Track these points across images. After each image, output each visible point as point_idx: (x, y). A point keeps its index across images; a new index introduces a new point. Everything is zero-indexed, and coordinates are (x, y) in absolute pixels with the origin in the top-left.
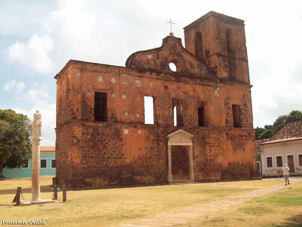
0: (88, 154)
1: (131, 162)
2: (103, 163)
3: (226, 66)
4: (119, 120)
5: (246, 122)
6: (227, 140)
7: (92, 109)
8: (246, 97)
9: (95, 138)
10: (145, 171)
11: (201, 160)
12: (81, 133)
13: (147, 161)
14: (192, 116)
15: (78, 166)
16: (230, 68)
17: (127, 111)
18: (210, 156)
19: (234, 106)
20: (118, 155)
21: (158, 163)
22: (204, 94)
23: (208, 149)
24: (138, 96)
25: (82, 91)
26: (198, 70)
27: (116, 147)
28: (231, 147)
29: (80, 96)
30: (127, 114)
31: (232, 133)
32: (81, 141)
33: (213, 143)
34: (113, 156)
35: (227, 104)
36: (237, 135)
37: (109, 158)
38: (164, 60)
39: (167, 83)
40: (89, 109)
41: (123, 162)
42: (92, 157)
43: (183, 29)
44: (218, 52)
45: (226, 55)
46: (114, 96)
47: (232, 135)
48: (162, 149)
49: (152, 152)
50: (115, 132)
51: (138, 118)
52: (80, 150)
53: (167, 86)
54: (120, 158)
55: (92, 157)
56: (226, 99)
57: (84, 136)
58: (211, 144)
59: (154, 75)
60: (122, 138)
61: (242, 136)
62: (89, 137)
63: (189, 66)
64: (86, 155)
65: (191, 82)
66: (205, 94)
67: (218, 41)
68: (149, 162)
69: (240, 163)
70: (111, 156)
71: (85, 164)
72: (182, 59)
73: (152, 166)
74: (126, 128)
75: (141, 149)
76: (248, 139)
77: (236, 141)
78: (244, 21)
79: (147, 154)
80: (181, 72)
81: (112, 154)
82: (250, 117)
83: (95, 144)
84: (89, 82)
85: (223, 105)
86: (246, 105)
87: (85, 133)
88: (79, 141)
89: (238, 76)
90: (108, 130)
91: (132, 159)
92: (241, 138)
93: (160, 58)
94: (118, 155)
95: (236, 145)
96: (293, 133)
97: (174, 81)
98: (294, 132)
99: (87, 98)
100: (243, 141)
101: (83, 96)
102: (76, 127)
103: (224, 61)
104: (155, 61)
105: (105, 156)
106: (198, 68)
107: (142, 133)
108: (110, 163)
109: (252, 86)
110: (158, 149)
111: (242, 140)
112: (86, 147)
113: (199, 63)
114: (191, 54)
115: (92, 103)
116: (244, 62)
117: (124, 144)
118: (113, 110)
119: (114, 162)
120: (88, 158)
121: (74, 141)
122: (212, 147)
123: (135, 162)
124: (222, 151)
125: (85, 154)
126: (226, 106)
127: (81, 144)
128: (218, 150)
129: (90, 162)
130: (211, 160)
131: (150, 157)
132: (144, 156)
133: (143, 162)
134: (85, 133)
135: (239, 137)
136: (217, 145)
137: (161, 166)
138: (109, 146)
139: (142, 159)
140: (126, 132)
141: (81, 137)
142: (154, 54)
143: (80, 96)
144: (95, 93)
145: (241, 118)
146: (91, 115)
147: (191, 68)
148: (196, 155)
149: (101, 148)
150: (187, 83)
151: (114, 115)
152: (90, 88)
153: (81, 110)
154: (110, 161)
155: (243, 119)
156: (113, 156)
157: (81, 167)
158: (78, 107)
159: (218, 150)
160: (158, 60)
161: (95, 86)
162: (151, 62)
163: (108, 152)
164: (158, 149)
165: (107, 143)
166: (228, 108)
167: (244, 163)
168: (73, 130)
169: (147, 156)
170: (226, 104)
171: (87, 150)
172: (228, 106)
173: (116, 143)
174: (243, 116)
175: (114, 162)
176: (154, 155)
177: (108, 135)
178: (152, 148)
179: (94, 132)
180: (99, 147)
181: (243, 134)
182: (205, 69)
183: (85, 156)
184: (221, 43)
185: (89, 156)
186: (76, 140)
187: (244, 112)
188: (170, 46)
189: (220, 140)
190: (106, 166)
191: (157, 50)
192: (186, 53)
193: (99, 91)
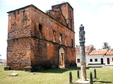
12: (34, 43)
54: (46, 57)
83: (39, 49)
162: (54, 16)
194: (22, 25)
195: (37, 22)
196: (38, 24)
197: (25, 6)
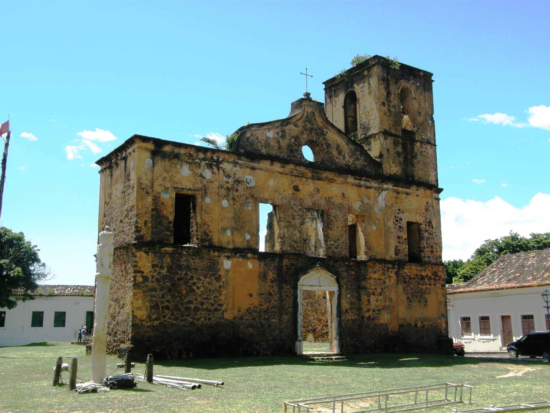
0: (162, 302)
1: (235, 318)
2: (186, 319)
3: (399, 154)
4: (216, 244)
5: (430, 253)
6: (397, 284)
7: (170, 222)
8: (430, 209)
9: (174, 273)
10: (258, 335)
11: (354, 318)
12: (150, 265)
13: (260, 316)
14: (338, 239)
15: (144, 323)
16: (405, 158)
17: (229, 228)
18: (368, 311)
19: (409, 224)
20: (212, 305)
21: (280, 320)
22: (359, 203)
23: (364, 298)
24: (249, 202)
25: (153, 191)
27: (210, 290)
28: (404, 297)
29: (150, 199)
30: (229, 233)
31: (405, 272)
32: (150, 279)
33: (372, 288)
34: (205, 307)
35: (398, 220)
36: (414, 276)
37: (197, 309)
38: (293, 140)
39: (297, 182)
40: (165, 222)
41: (220, 318)
42: (167, 308)
43: (324, 83)
45: (398, 134)
46: (208, 200)
47: (405, 276)
48: (287, 296)
49: (270, 301)
50: (209, 264)
51: (248, 241)
52: (148, 294)
53: (297, 186)
54: (216, 310)
55: (167, 308)
56: (397, 211)
57: (155, 270)
58: (370, 290)
59: (277, 167)
60: (220, 276)
61: (423, 278)
62: (164, 272)
63: (335, 153)
64: (157, 304)
65: (340, 179)
66: (362, 202)
67: (386, 109)
68: (264, 318)
69: (419, 325)
70: (200, 306)
71: (155, 319)
72: (324, 139)
73: (269, 326)
74: (228, 258)
75: (251, 295)
76: (432, 283)
77: (412, 286)
78: (432, 75)
79: (261, 305)
80: (322, 162)
81: (202, 304)
82: (437, 244)
83: (173, 285)
84: (167, 176)
85: (392, 222)
86: (430, 222)
87: (157, 266)
88: (145, 279)
89: (419, 173)
90: (197, 260)
91: (236, 313)
92: (422, 282)
93: (288, 137)
94: (212, 305)
95: (412, 293)
96: (510, 275)
97: (310, 178)
98: (512, 273)
99: (162, 204)
100: (424, 287)
101: (156, 199)
102: (142, 253)
103: (396, 144)
104: (279, 142)
105: (189, 306)
106: (350, 157)
107: (253, 268)
108: (198, 320)
109: (441, 190)
110: (281, 296)
111: (423, 284)
112: (158, 290)
113: (353, 147)
114: (339, 131)
115: (170, 213)
116: (429, 147)
117: (224, 287)
118: (206, 226)
119: (205, 317)
120: (161, 309)
121: (137, 278)
122: (372, 296)
123: (242, 318)
124: (388, 303)
125: (155, 301)
126: (396, 225)
127: (150, 284)
128: (381, 300)
129: (164, 317)
130: (369, 318)
131: (266, 311)
132: (256, 308)
133: (255, 318)
134: (157, 266)
135: (418, 278)
136: (381, 293)
137: (285, 327)
138: (198, 288)
139: (254, 314)
140: (227, 264)
141: (150, 272)
142: (278, 130)
143: (151, 200)
144: (176, 194)
145: (422, 245)
146: (169, 233)
147: (338, 156)
148: (344, 309)
149: (184, 292)
150: (331, 181)
151: (208, 235)
153: (152, 224)
154: (199, 316)
155: (424, 248)
156: (205, 307)
157: (149, 325)
158: (146, 219)
159: (381, 300)
161: (177, 183)
162: (273, 143)
163: (196, 299)
164: (281, 296)
165: (194, 284)
166: (400, 227)
167: (426, 326)
168: (137, 259)
169: (261, 307)
170: (397, 221)
171: (160, 296)
172: (399, 224)
173: (209, 283)
174: (425, 242)
175: (205, 317)
176: (274, 307)
177: (196, 269)
178: (270, 294)
179: (173, 264)
180: (181, 290)
181: (424, 274)
183: (156, 306)
184: (390, 113)
185: (163, 305)
186: (142, 276)
187: (427, 235)
188: (305, 116)
189: (385, 283)
190: (192, 323)
191: (282, 123)
192: (331, 128)
193: (185, 192)
196: (174, 196)
197: (123, 142)
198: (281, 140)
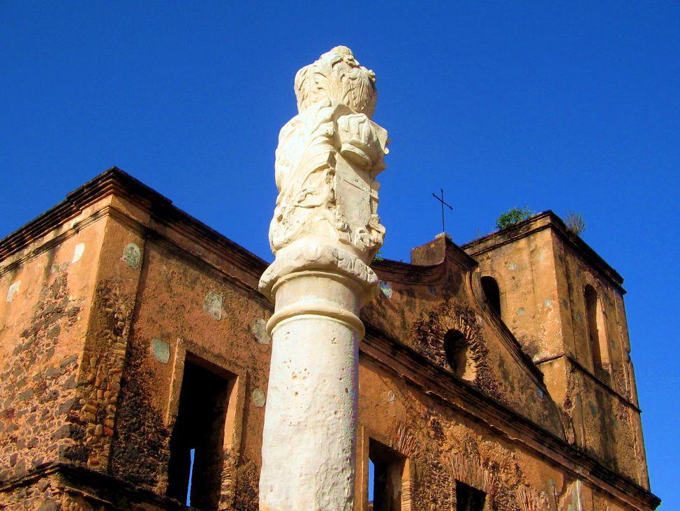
7: (164, 433)
16: (602, 419)
26: (524, 397)
38: (427, 318)
44: (571, 353)
63: (497, 372)
99: (151, 374)
147: (502, 381)
150: (495, 434)
152: (171, 330)
160: (410, 310)
182: (541, 400)
194: (19, 370)
195: (166, 338)
198: (406, 309)
